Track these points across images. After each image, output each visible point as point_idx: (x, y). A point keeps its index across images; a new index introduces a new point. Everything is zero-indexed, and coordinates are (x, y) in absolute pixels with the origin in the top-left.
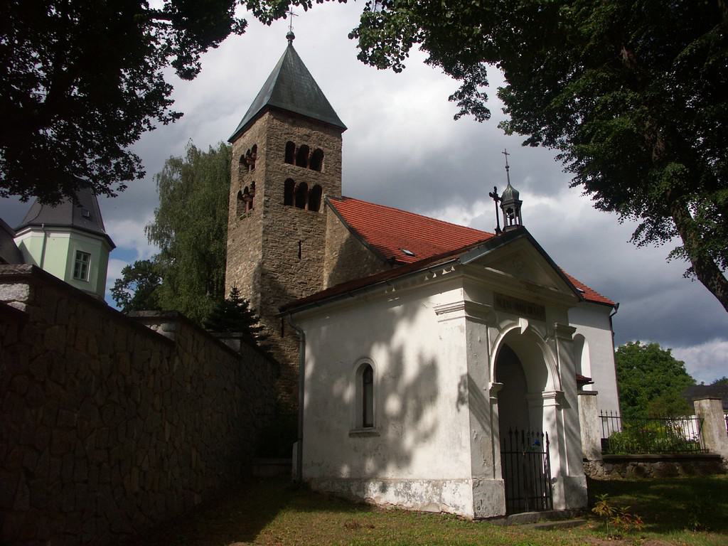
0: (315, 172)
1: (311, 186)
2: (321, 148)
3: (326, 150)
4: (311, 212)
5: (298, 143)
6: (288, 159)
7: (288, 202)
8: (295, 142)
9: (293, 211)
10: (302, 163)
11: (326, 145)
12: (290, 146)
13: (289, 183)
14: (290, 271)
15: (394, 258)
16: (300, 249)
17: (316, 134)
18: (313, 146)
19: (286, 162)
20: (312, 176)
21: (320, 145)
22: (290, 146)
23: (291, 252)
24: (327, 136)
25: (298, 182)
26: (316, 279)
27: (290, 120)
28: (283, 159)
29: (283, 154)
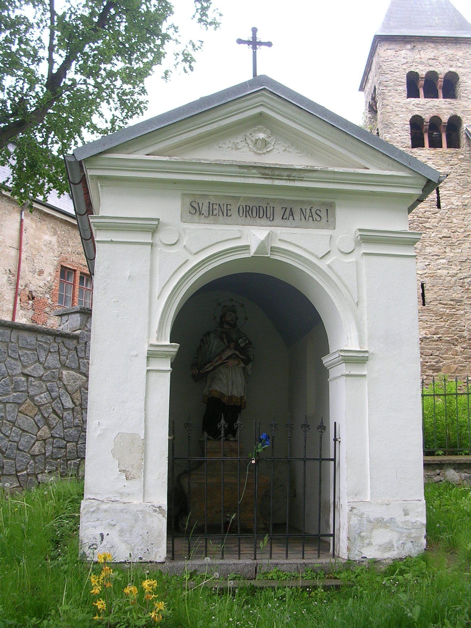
0: (448, 100)
1: (445, 119)
2: (452, 70)
3: (459, 71)
5: (422, 71)
6: (412, 92)
8: (417, 71)
10: (431, 93)
11: (460, 65)
14: (427, 225)
16: (438, 198)
18: (442, 70)
19: (409, 96)
20: (444, 106)
21: (451, 66)
24: (460, 54)
25: (427, 117)
26: (462, 230)
27: (409, 46)
28: (405, 94)
29: (404, 88)
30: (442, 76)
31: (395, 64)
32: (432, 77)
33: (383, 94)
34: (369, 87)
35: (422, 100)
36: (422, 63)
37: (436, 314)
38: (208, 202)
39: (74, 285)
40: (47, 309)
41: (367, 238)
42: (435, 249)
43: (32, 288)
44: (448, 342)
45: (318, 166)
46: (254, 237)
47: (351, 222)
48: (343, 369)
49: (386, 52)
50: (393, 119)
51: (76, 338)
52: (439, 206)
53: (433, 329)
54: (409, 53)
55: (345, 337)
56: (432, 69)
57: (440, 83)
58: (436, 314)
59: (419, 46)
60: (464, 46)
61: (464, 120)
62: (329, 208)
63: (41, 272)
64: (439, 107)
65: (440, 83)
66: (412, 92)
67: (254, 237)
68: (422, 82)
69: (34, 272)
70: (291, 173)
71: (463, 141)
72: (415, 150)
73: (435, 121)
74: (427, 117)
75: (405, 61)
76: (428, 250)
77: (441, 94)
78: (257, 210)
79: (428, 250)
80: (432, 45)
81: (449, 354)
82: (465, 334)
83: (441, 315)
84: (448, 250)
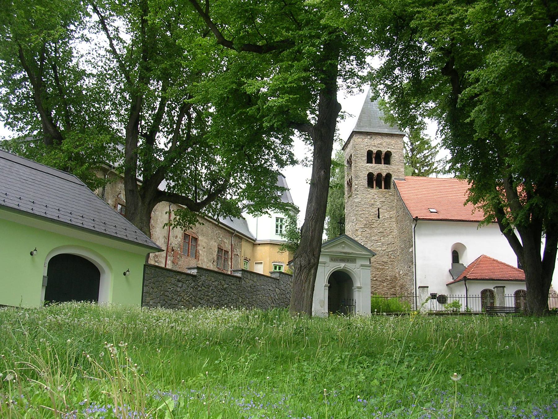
1: (384, 175)
2: (389, 150)
3: (392, 151)
4: (385, 190)
5: (375, 150)
6: (369, 161)
7: (370, 185)
9: (375, 190)
10: (378, 161)
12: (370, 153)
13: (370, 176)
14: (373, 226)
15: (417, 217)
17: (387, 140)
22: (370, 153)
23: (373, 215)
24: (393, 142)
25: (375, 174)
27: (369, 137)
30: (384, 153)
31: (362, 146)
32: (379, 153)
33: (356, 161)
34: (348, 150)
35: (374, 165)
36: (375, 146)
37: (375, 268)
38: (334, 259)
39: (189, 243)
40: (178, 256)
41: (362, 266)
42: (376, 238)
43: (173, 245)
44: (380, 281)
45: (354, 252)
46: (342, 265)
47: (359, 262)
48: (357, 289)
49: (357, 139)
50: (360, 174)
51: (278, 280)
52: (379, 217)
53: (374, 275)
54: (369, 140)
55: (357, 284)
56: (379, 149)
57: (383, 156)
58: (375, 268)
59: (374, 137)
60: (395, 138)
61: (393, 175)
62: (355, 260)
63: (177, 237)
64: (381, 169)
65: (383, 156)
66: (369, 161)
67: (342, 265)
68: (374, 156)
69: (173, 237)
70: (349, 253)
71: (392, 186)
72: (369, 189)
73: (379, 175)
74: (375, 174)
75: (367, 144)
76: (373, 238)
77: (383, 162)
78: (343, 260)
79: (373, 238)
80: (380, 137)
81: (381, 287)
82: (388, 278)
83: (378, 269)
84: (382, 238)
